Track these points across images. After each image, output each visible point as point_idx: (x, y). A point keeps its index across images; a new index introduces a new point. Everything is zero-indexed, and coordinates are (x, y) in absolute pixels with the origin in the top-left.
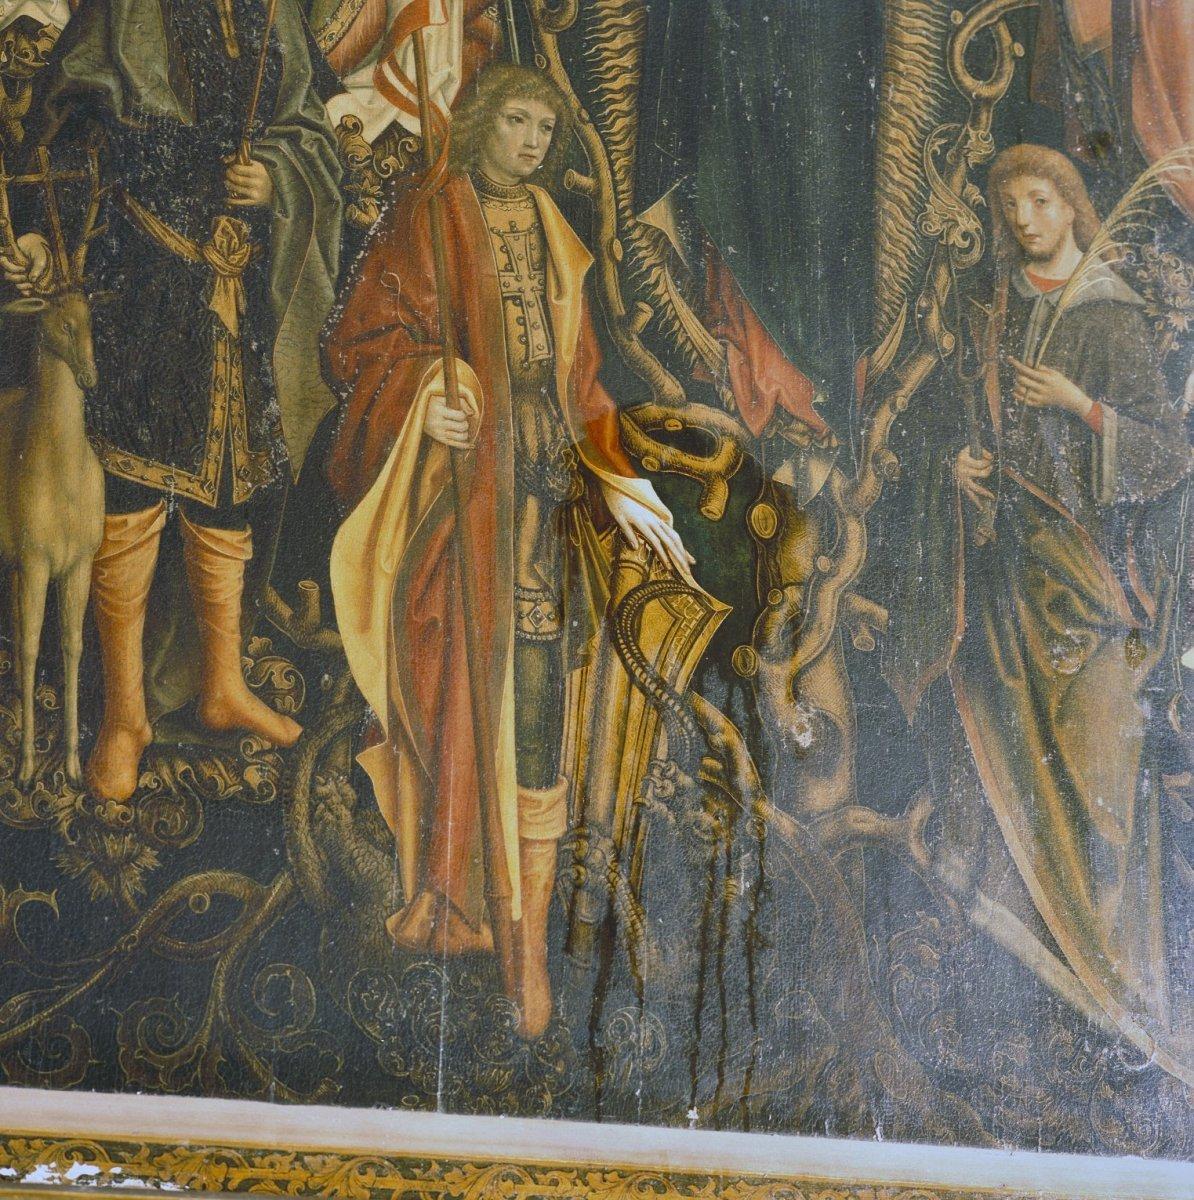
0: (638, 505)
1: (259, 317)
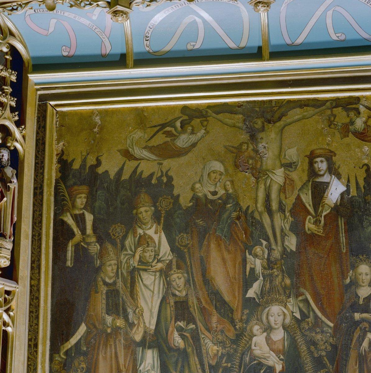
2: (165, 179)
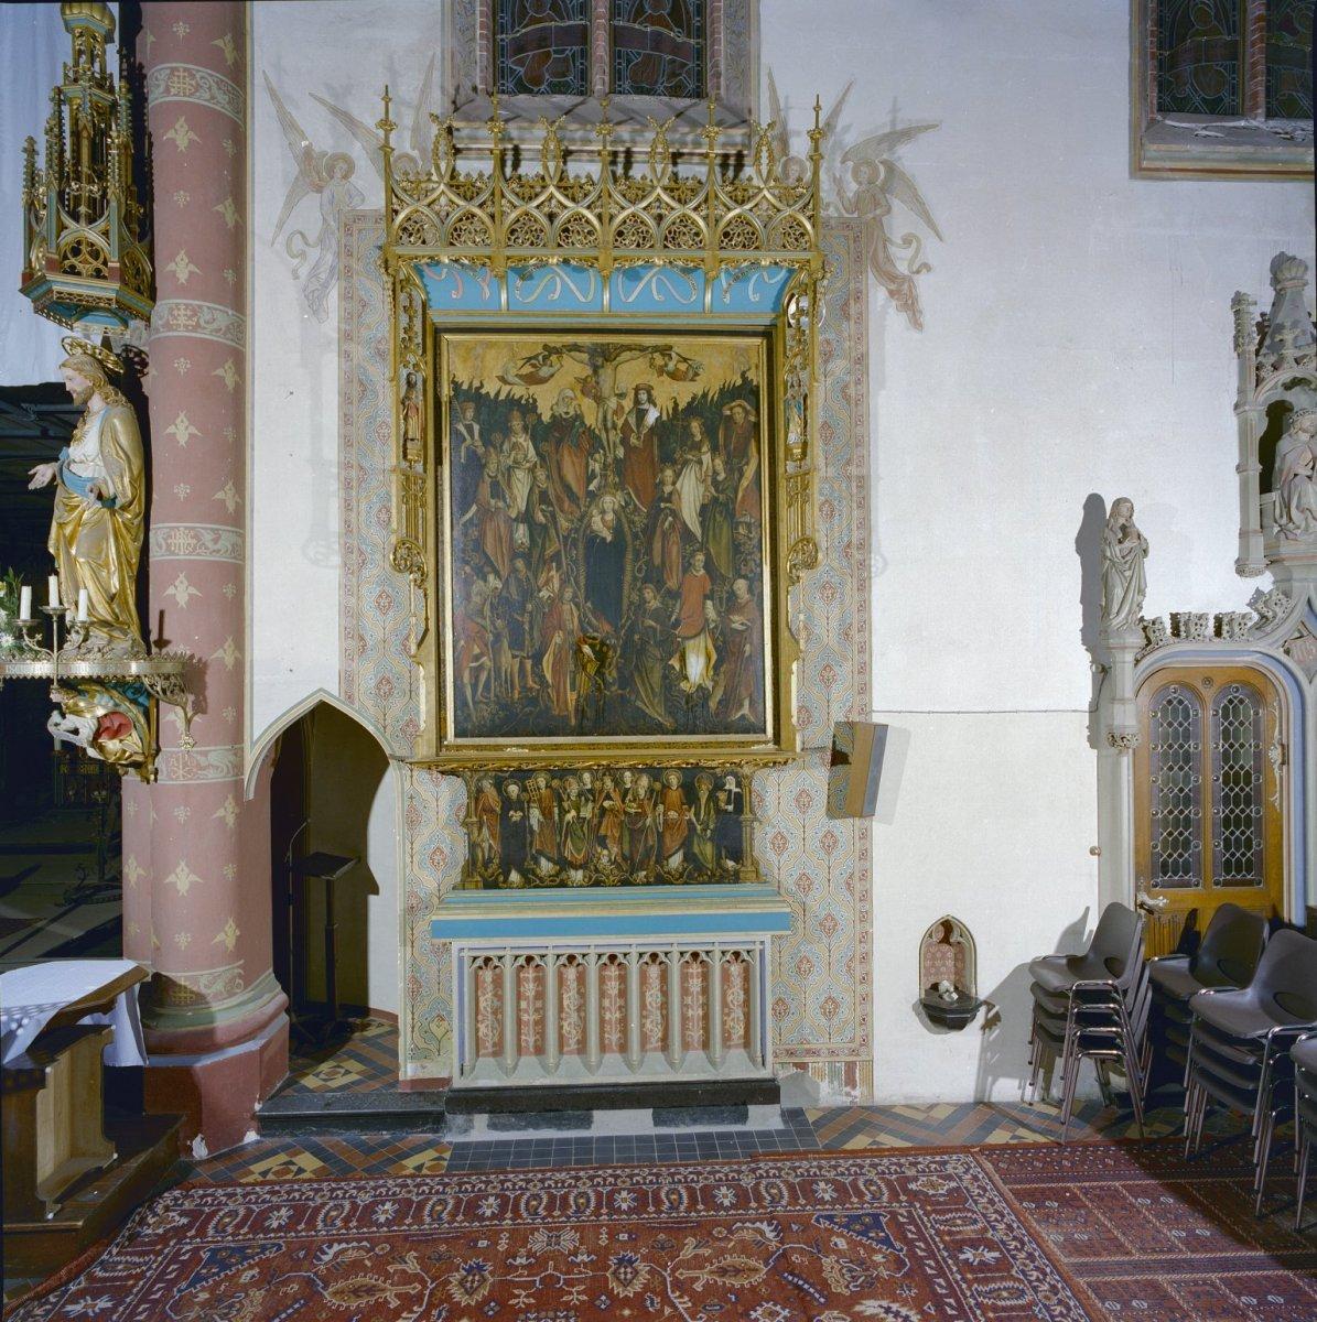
0: (587, 649)
1: (531, 628)
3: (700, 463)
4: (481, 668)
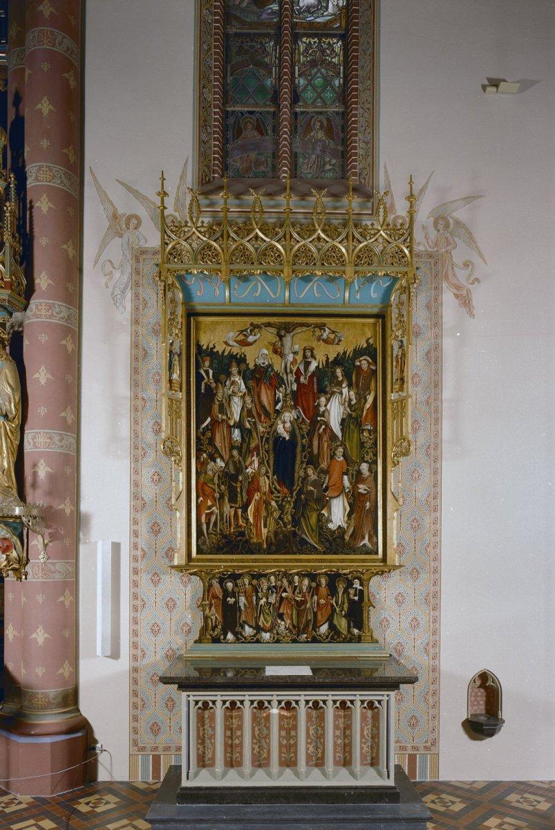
1: (241, 490)
2: (243, 356)
3: (341, 393)
4: (212, 513)
